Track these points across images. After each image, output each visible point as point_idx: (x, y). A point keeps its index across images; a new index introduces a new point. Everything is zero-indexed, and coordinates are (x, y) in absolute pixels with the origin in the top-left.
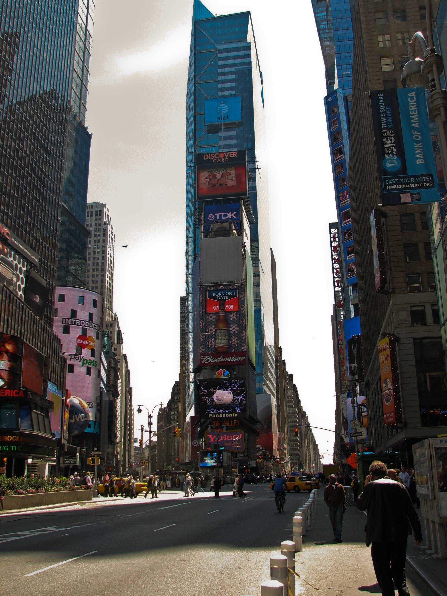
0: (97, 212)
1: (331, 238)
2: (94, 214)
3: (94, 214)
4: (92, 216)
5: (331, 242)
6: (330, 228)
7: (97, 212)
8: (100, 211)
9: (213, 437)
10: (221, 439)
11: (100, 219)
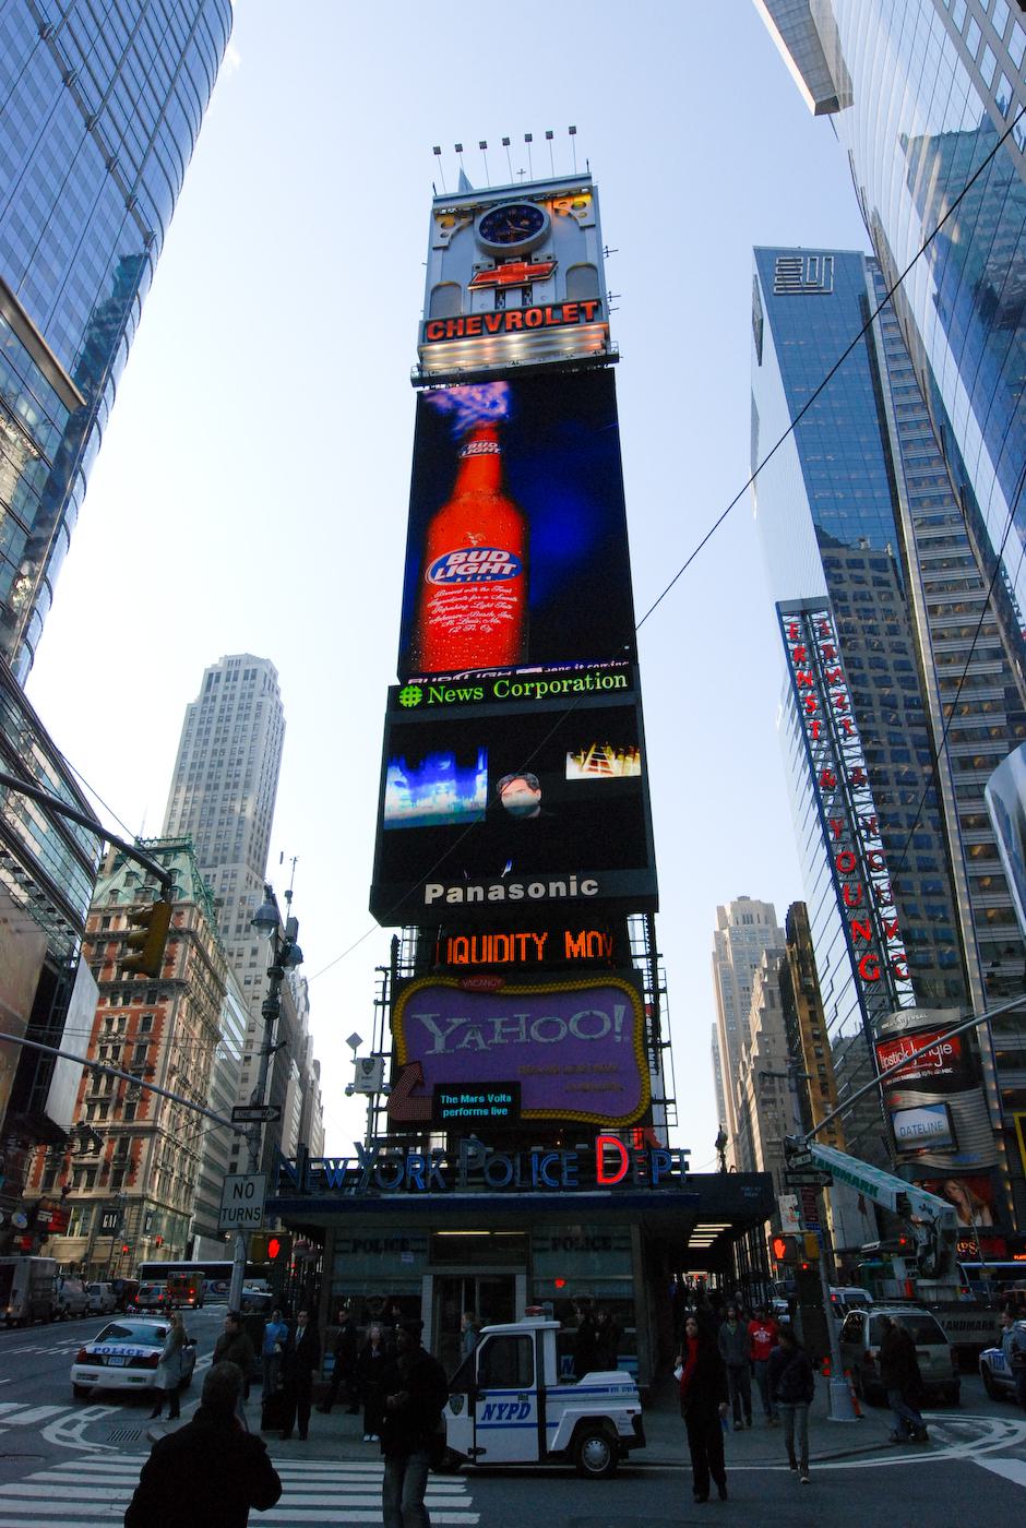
0: (247, 671)
1: (784, 633)
2: (241, 676)
3: (241, 676)
4: (235, 679)
5: (785, 642)
6: (780, 615)
7: (247, 671)
8: (255, 671)
9: (442, 1025)
10: (497, 1039)
11: (252, 686)
